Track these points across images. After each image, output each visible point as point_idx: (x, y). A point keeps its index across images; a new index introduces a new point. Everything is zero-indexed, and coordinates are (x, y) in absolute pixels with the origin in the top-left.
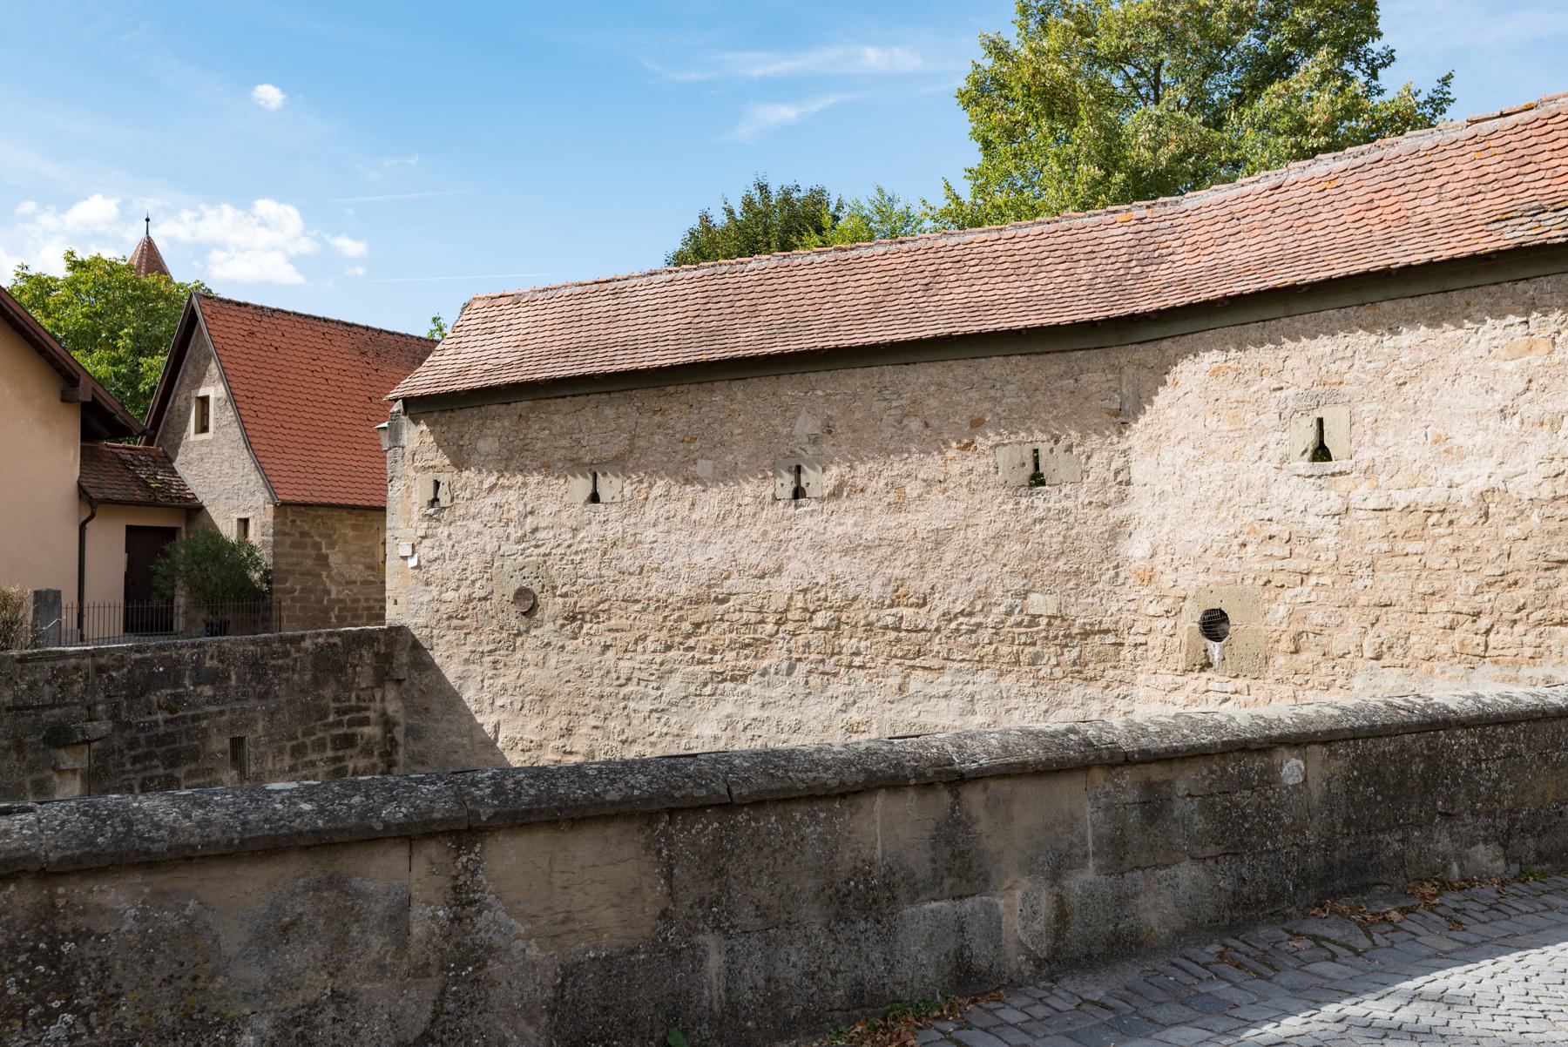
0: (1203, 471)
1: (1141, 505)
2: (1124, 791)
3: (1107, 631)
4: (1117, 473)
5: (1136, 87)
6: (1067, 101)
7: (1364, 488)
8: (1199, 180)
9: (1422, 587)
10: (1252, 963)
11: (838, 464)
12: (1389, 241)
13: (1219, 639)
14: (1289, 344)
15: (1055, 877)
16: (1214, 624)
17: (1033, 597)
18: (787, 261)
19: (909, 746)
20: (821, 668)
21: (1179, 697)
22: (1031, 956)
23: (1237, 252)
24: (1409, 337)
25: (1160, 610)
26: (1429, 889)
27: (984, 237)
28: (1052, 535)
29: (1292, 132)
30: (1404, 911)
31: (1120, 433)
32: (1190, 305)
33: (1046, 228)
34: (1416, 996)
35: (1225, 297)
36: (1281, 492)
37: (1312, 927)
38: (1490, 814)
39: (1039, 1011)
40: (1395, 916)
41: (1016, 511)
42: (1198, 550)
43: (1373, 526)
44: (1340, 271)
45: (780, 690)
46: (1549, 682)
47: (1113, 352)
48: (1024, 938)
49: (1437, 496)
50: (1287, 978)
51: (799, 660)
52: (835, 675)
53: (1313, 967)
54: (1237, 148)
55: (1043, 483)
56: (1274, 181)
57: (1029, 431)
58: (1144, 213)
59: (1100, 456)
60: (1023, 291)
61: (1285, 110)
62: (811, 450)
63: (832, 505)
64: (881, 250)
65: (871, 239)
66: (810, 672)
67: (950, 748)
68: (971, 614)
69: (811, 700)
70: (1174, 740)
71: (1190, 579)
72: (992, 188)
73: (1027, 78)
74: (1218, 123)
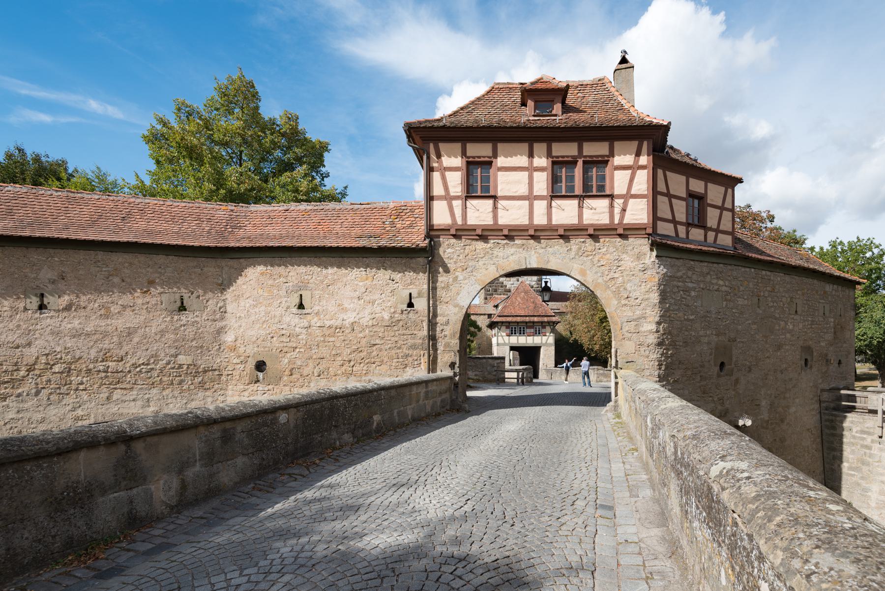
0: (257, 310)
1: (231, 321)
2: (214, 433)
3: (215, 370)
4: (220, 308)
5: (232, 158)
6: (199, 154)
7: (316, 319)
8: (258, 200)
9: (334, 352)
10: (265, 488)
11: (69, 295)
12: (325, 237)
13: (262, 371)
14: (290, 267)
15: (180, 472)
16: (260, 366)
17: (180, 357)
18: (34, 191)
19: (101, 427)
20: (58, 391)
21: (246, 394)
22: (167, 505)
23: (271, 231)
24: (331, 270)
25: (238, 361)
26: (329, 451)
27: (156, 202)
28: (190, 332)
29: (294, 192)
30: (320, 459)
31: (222, 293)
32: (252, 247)
33: (188, 205)
34: (322, 487)
35: (266, 247)
36: (287, 319)
37: (289, 471)
38: (349, 424)
39: (172, 527)
40: (317, 461)
41: (172, 321)
42: (255, 339)
43: (318, 332)
44: (308, 244)
45: (30, 404)
46: (370, 381)
47: (219, 261)
48: (164, 499)
49: (338, 323)
50: (277, 491)
51: (44, 388)
52: (67, 394)
53: (288, 485)
54: (273, 192)
55: (185, 310)
56: (285, 208)
57: (179, 288)
58: (233, 208)
59: (213, 302)
60: (176, 229)
61: (291, 183)
62: (50, 287)
63: (65, 314)
64: (97, 197)
65: (93, 190)
66: (51, 394)
67: (125, 426)
68: (148, 364)
69: (52, 407)
70: (236, 412)
71: (251, 350)
72: (162, 181)
73: (178, 139)
74: (266, 181)
